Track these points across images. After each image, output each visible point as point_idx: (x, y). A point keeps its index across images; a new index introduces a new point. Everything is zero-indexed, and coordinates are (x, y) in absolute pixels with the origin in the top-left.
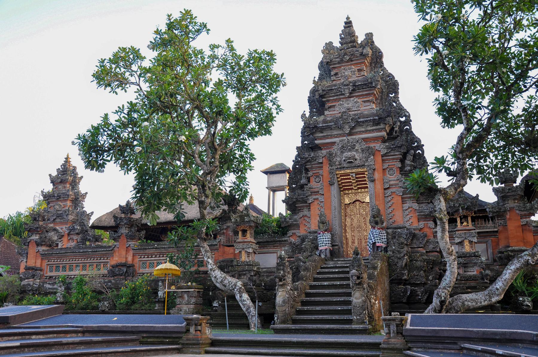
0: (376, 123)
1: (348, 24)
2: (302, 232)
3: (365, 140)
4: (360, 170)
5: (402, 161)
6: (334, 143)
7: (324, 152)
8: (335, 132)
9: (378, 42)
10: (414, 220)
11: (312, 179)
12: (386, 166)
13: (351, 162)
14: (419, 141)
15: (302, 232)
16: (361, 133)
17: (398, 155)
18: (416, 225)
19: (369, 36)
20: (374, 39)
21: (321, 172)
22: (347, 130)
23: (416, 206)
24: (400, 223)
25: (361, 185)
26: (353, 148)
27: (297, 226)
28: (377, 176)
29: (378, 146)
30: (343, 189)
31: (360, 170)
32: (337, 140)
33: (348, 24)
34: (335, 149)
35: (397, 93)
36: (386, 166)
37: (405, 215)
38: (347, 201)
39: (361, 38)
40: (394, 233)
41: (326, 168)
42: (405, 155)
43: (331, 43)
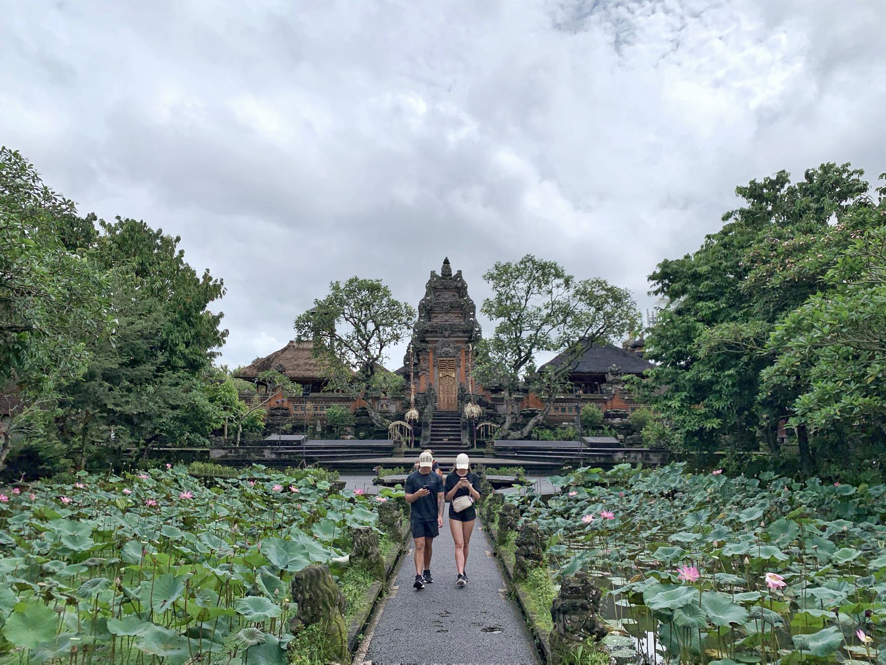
0: (464, 332)
1: (446, 262)
6: (437, 341)
9: (465, 277)
13: (447, 354)
19: (460, 272)
20: (463, 275)
32: (441, 339)
33: (446, 262)
34: (438, 345)
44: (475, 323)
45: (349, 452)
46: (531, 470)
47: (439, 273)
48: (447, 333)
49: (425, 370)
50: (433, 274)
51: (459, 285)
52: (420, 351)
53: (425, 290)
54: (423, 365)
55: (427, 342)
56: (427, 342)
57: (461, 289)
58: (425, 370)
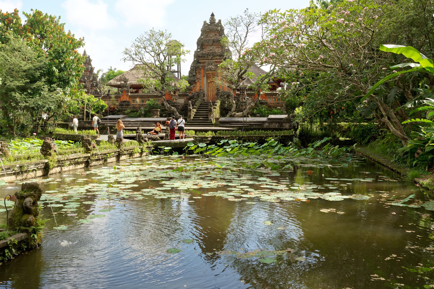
19: (220, 21)
39: (217, 21)
41: (202, 70)
45: (137, 124)
48: (210, 57)
49: (199, 79)
52: (197, 68)
53: (200, 33)
54: (198, 76)
57: (221, 32)
58: (199, 79)
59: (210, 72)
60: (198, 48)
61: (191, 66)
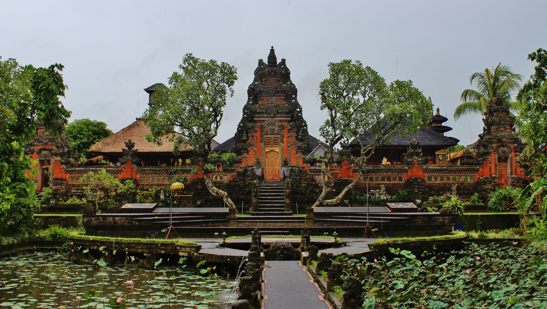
0: (287, 113)
1: (272, 51)
2: (243, 165)
3: (280, 121)
4: (276, 136)
5: (297, 133)
6: (264, 121)
7: (258, 124)
8: (265, 115)
10: (301, 163)
11: (250, 138)
12: (289, 134)
14: (305, 123)
15: (243, 165)
16: (278, 117)
17: (296, 130)
18: (301, 166)
19: (284, 61)
21: (256, 135)
22: (272, 115)
23: (302, 156)
24: (295, 164)
25: (276, 143)
26: (274, 124)
27: (240, 162)
28: (285, 140)
29: (286, 124)
30: (267, 144)
31: (276, 136)
33: (272, 51)
35: (296, 95)
36: (289, 134)
37: (297, 161)
38: (267, 150)
39: (279, 61)
40: (292, 169)
42: (298, 131)
43: (262, 60)
44: (297, 105)
46: (343, 233)
47: (266, 61)
50: (261, 62)
51: (283, 71)
55: (256, 122)
56: (256, 122)
57: (286, 75)
59: (270, 136)
60: (249, 99)
61: (239, 126)
